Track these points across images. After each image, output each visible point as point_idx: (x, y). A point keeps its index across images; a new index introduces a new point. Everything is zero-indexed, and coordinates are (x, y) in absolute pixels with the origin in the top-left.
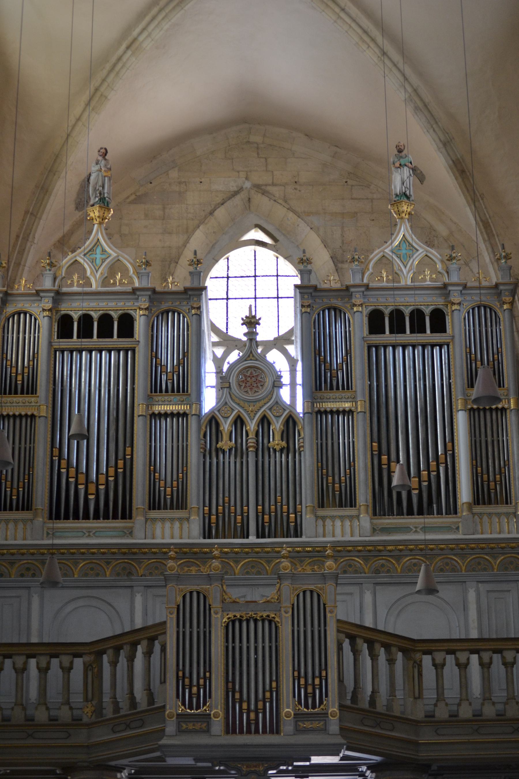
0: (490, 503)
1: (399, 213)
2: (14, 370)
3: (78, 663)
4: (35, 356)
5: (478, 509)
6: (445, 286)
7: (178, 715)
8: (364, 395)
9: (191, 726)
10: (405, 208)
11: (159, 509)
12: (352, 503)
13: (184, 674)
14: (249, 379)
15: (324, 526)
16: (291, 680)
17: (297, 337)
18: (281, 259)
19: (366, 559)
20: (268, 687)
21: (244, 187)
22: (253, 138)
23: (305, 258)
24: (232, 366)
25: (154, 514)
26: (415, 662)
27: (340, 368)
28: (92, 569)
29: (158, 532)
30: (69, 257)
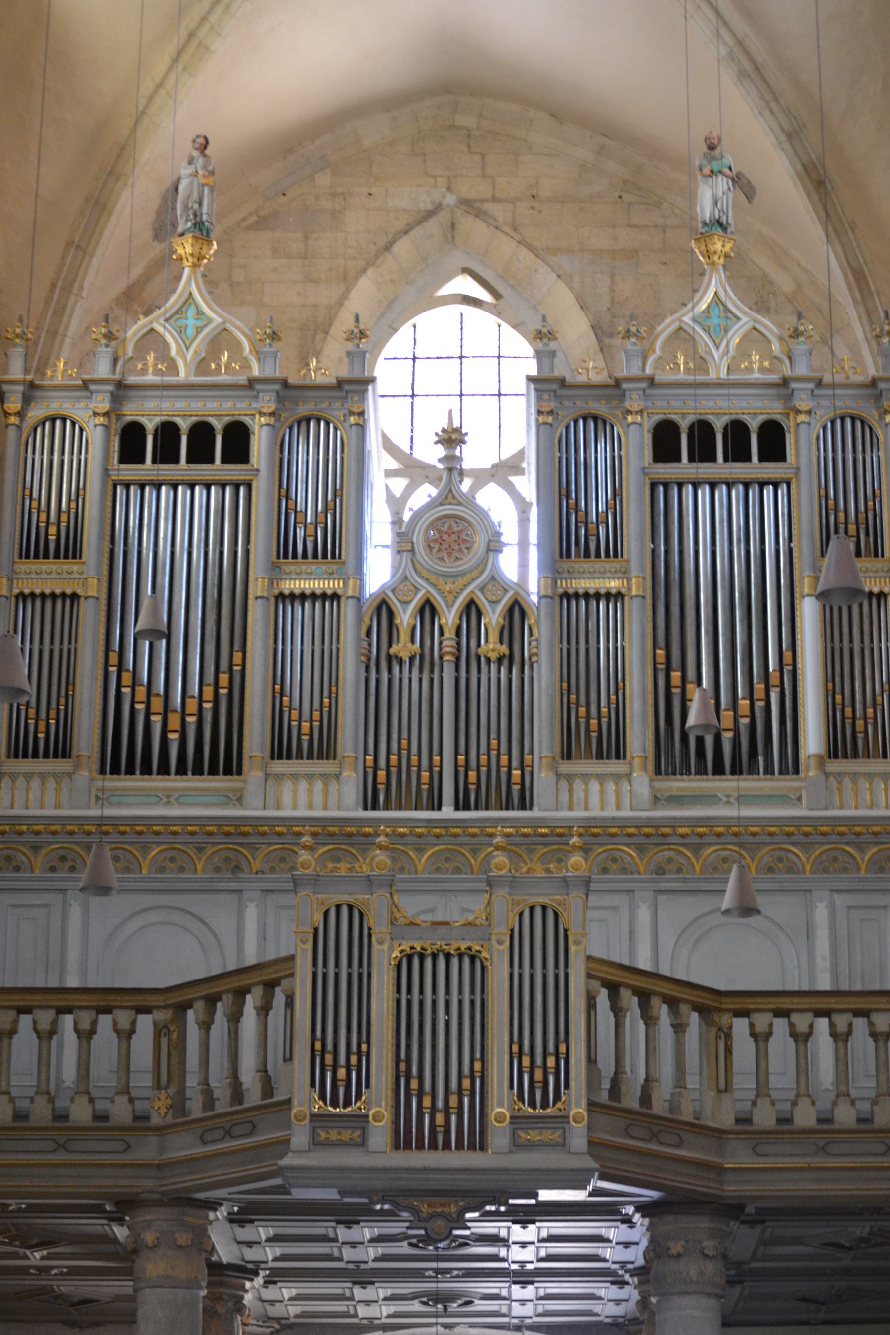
0: (856, 755)
1: (708, 255)
2: (43, 517)
3: (145, 1023)
4: (79, 493)
5: (834, 766)
6: (785, 382)
7: (313, 1116)
9: (334, 1135)
10: (718, 246)
11: (289, 757)
12: (620, 753)
14: (445, 537)
15: (571, 791)
16: (507, 1058)
17: (530, 463)
18: (506, 327)
19: (641, 849)
20: (466, 1070)
21: (444, 203)
22: (462, 120)
23: (545, 330)
24: (418, 515)
25: (280, 767)
26: (720, 1029)
27: (602, 519)
28: (172, 860)
29: (287, 798)
30: (140, 323)
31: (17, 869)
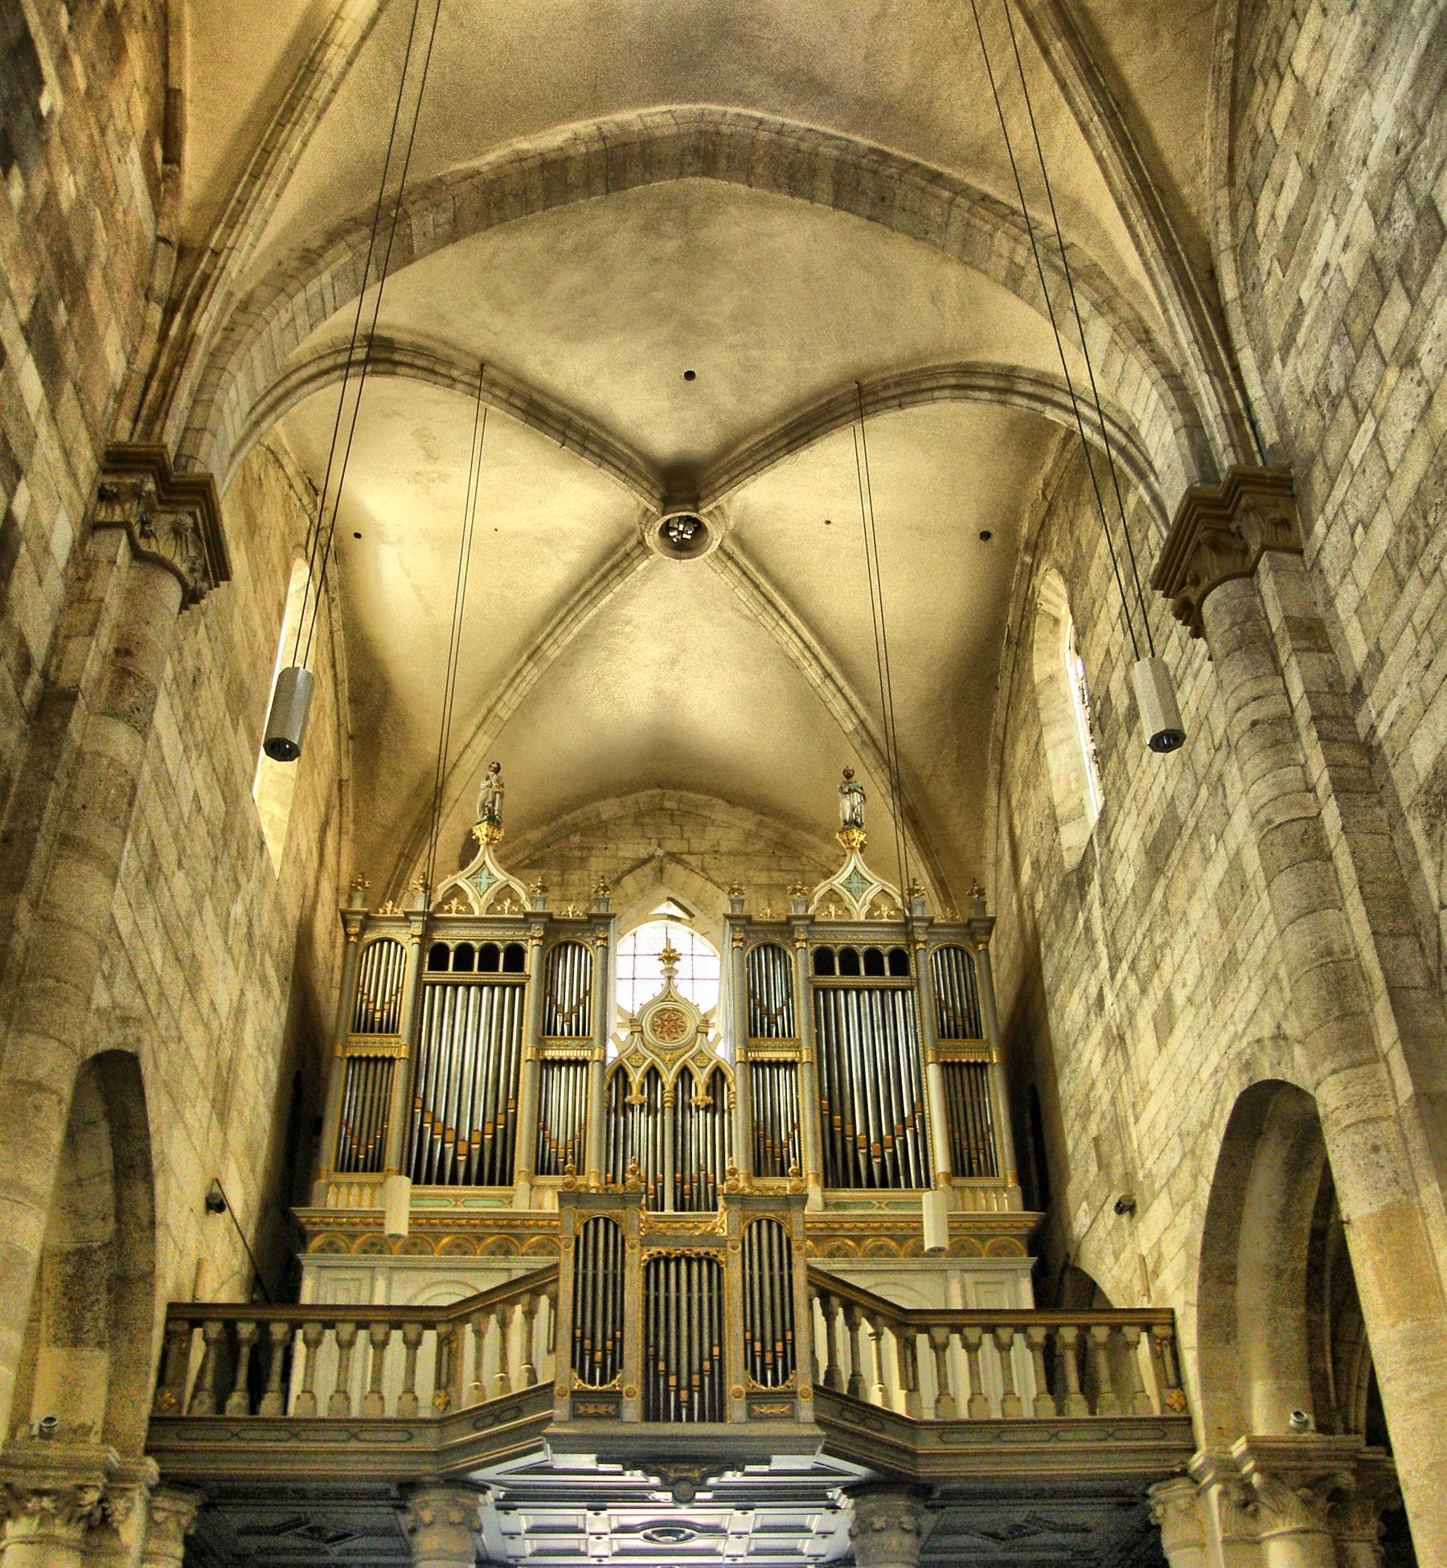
0: (971, 1174)
3: (430, 1337)
5: (959, 1181)
7: (574, 1393)
8: (810, 1043)
11: (549, 1173)
13: (583, 1333)
18: (697, 935)
20: (706, 1355)
22: (667, 804)
25: (543, 1180)
31: (337, 1251)
